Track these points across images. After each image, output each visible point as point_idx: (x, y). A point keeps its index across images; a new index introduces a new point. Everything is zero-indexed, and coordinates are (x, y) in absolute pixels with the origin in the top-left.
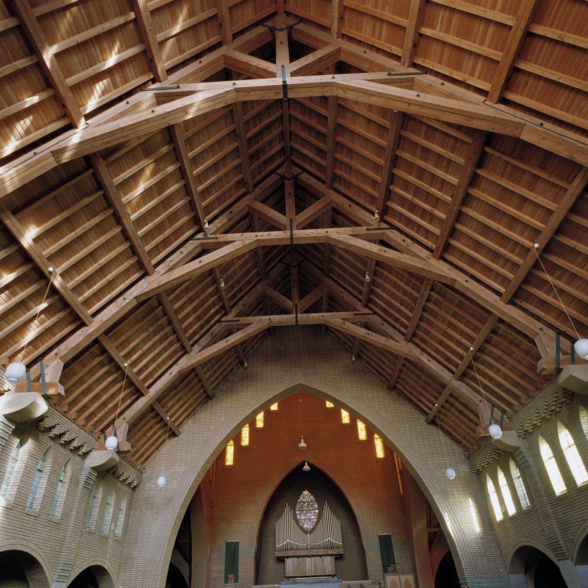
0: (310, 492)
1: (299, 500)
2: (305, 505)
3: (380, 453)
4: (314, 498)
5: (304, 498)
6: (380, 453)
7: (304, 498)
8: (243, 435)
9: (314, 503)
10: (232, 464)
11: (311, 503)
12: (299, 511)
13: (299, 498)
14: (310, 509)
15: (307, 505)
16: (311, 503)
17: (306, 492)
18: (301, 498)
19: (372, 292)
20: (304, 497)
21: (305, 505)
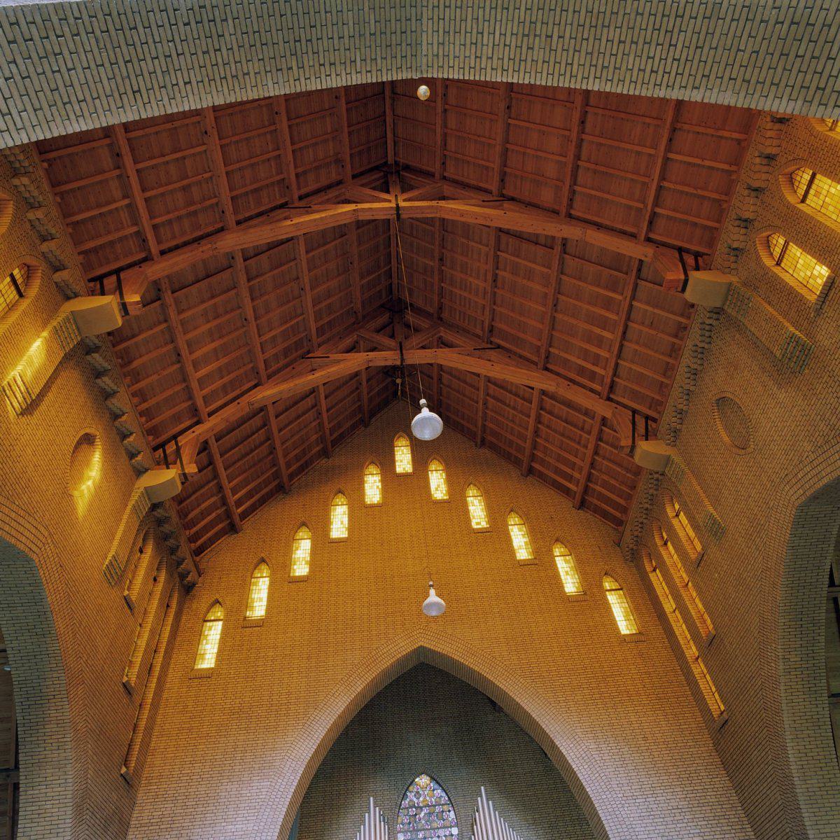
0: (433, 778)
1: (406, 803)
2: (422, 814)
3: (624, 624)
4: (444, 794)
5: (418, 794)
6: (624, 624)
7: (418, 794)
8: (255, 596)
9: (446, 808)
10: (213, 666)
11: (437, 809)
12: (405, 832)
13: (404, 796)
14: (435, 825)
15: (430, 814)
16: (437, 809)
17: (423, 780)
18: (411, 795)
19: (533, 457)
20: (418, 792)
21: (422, 814)
